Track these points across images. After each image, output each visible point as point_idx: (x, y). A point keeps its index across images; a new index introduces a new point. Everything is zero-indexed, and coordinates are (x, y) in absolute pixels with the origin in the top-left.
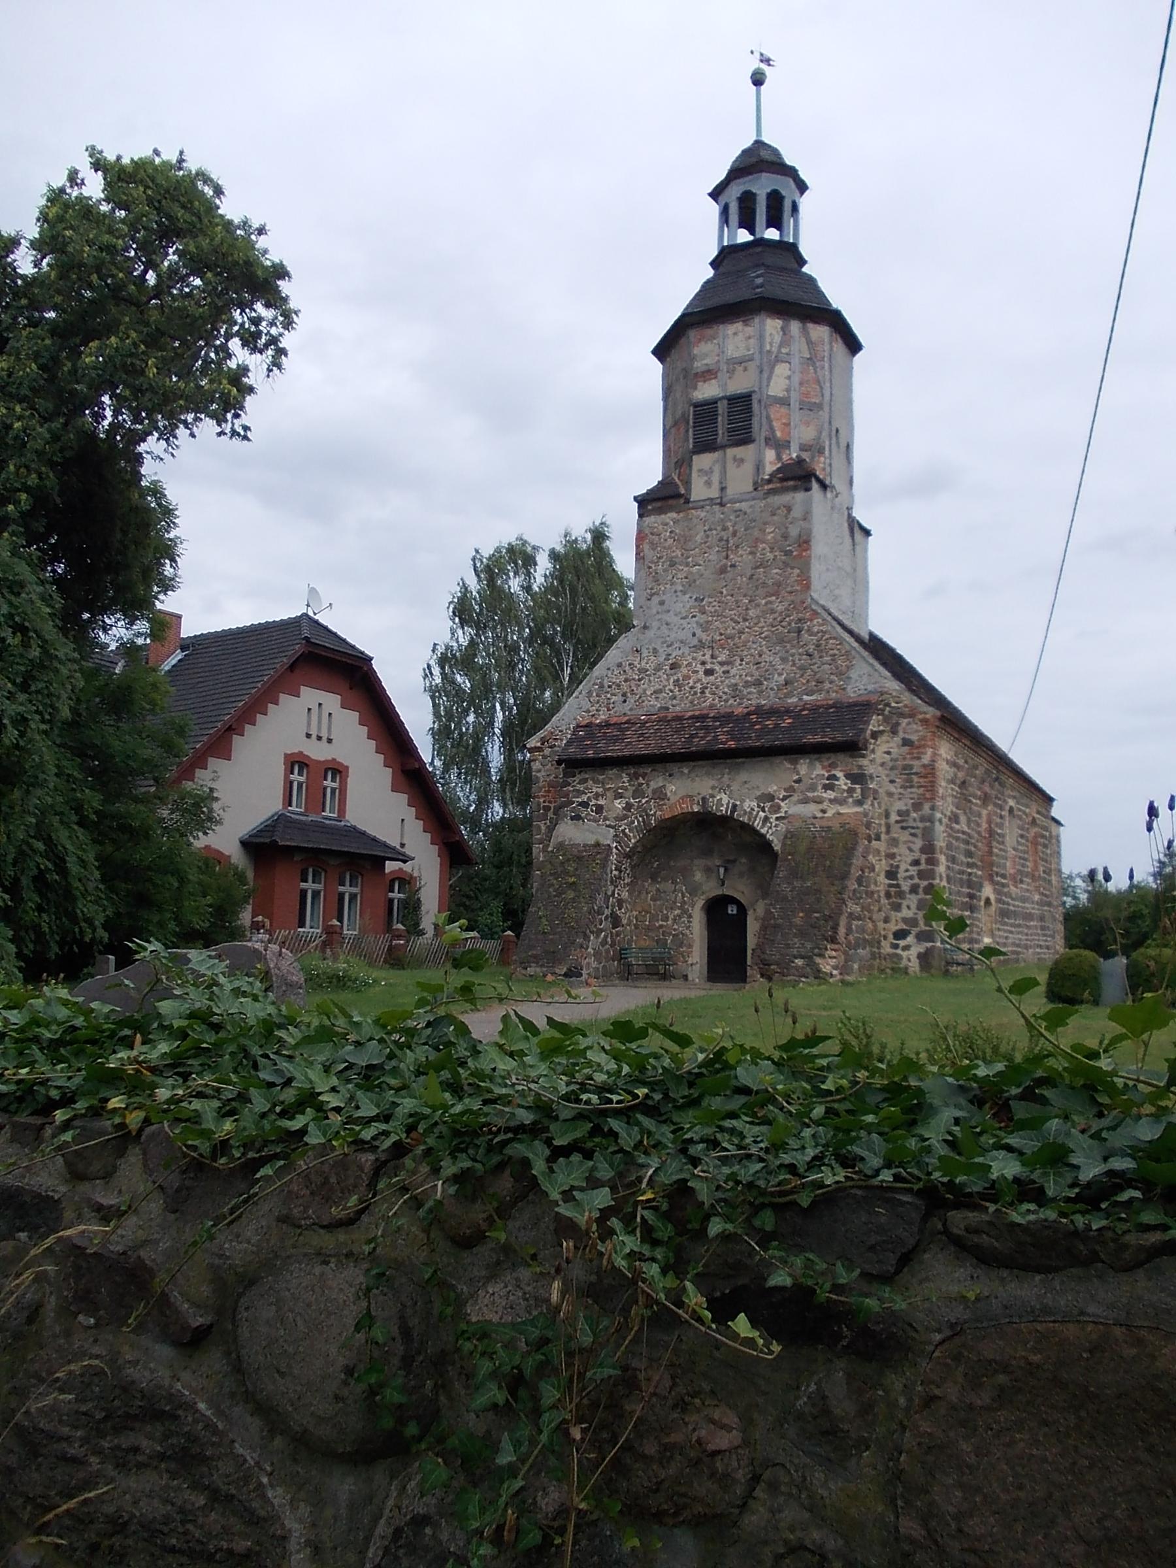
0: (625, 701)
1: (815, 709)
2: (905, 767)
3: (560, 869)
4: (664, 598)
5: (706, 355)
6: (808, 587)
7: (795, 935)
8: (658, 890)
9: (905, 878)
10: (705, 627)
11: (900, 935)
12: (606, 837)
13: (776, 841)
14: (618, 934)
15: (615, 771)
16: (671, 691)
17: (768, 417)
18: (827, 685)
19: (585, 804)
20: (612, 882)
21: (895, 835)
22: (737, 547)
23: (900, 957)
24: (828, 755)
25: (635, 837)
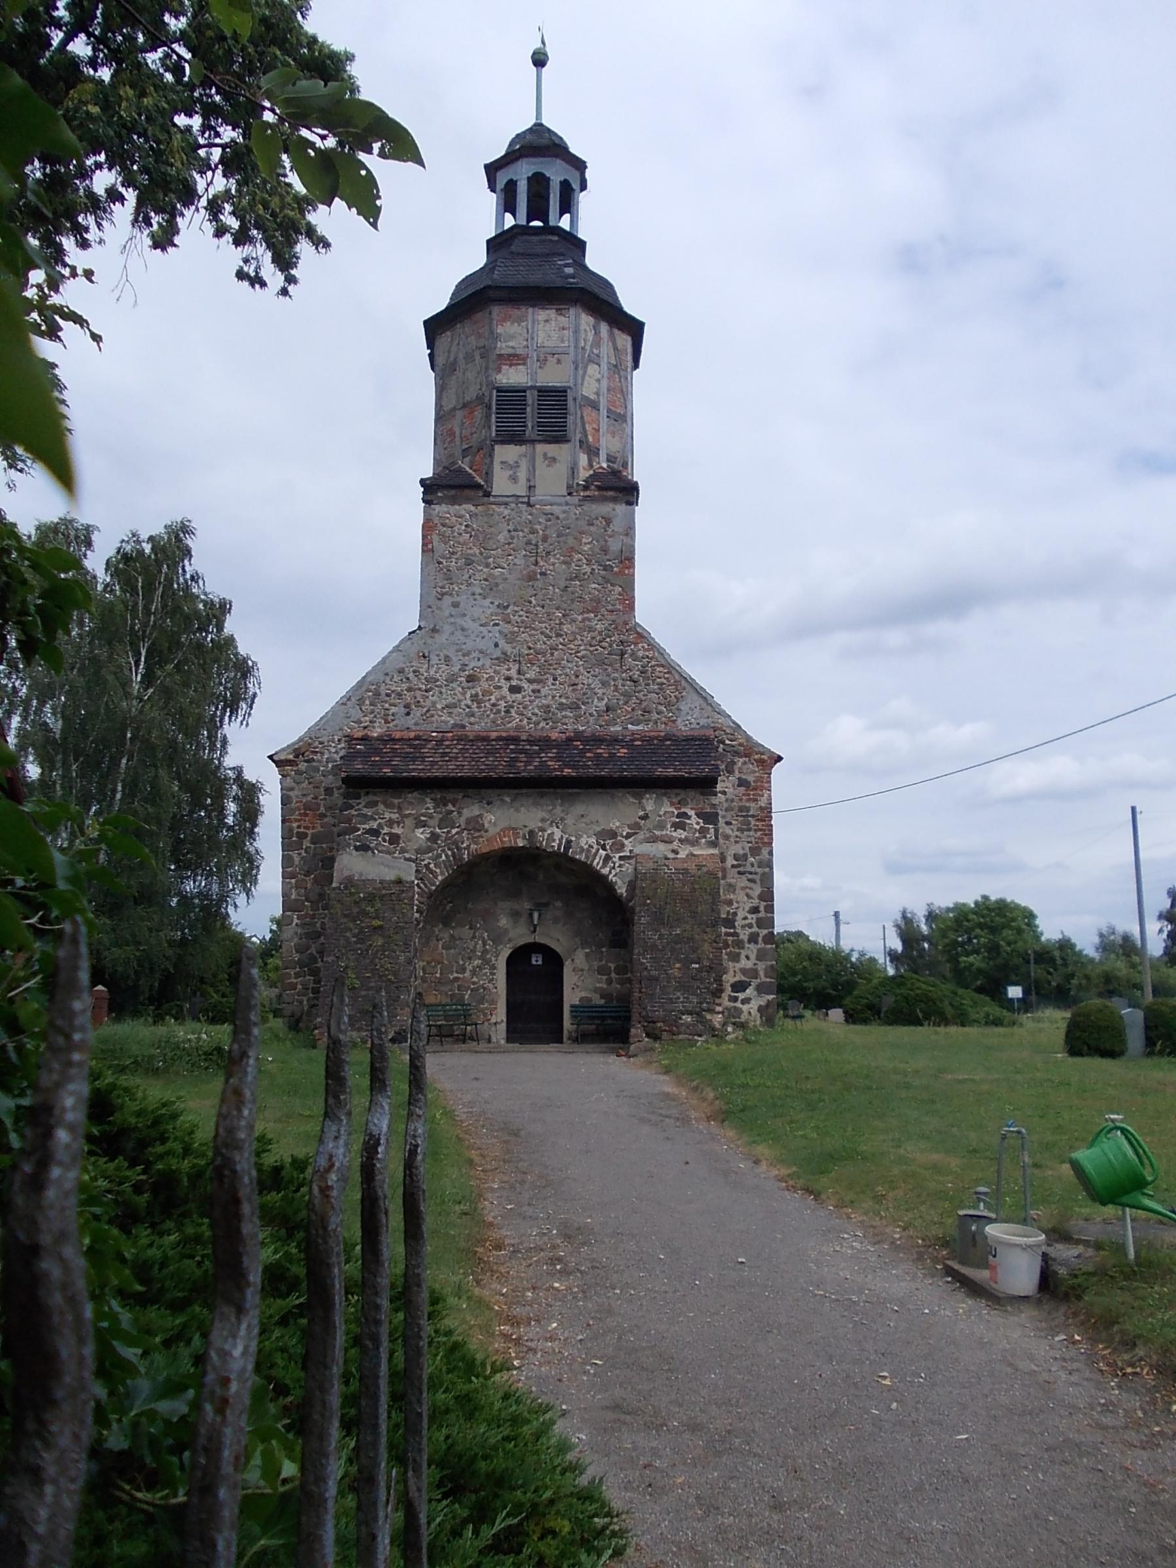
0: (408, 714)
1: (647, 740)
2: (741, 809)
3: (355, 910)
4: (458, 599)
5: (512, 337)
6: (631, 607)
7: (676, 989)
8: (452, 936)
9: (743, 927)
10: (511, 638)
11: (739, 987)
12: (410, 875)
13: (619, 882)
15: (415, 794)
16: (469, 707)
17: (582, 417)
18: (655, 716)
19: (375, 833)
21: (733, 881)
22: (548, 553)
23: (740, 1011)
24: (677, 791)
25: (442, 873)
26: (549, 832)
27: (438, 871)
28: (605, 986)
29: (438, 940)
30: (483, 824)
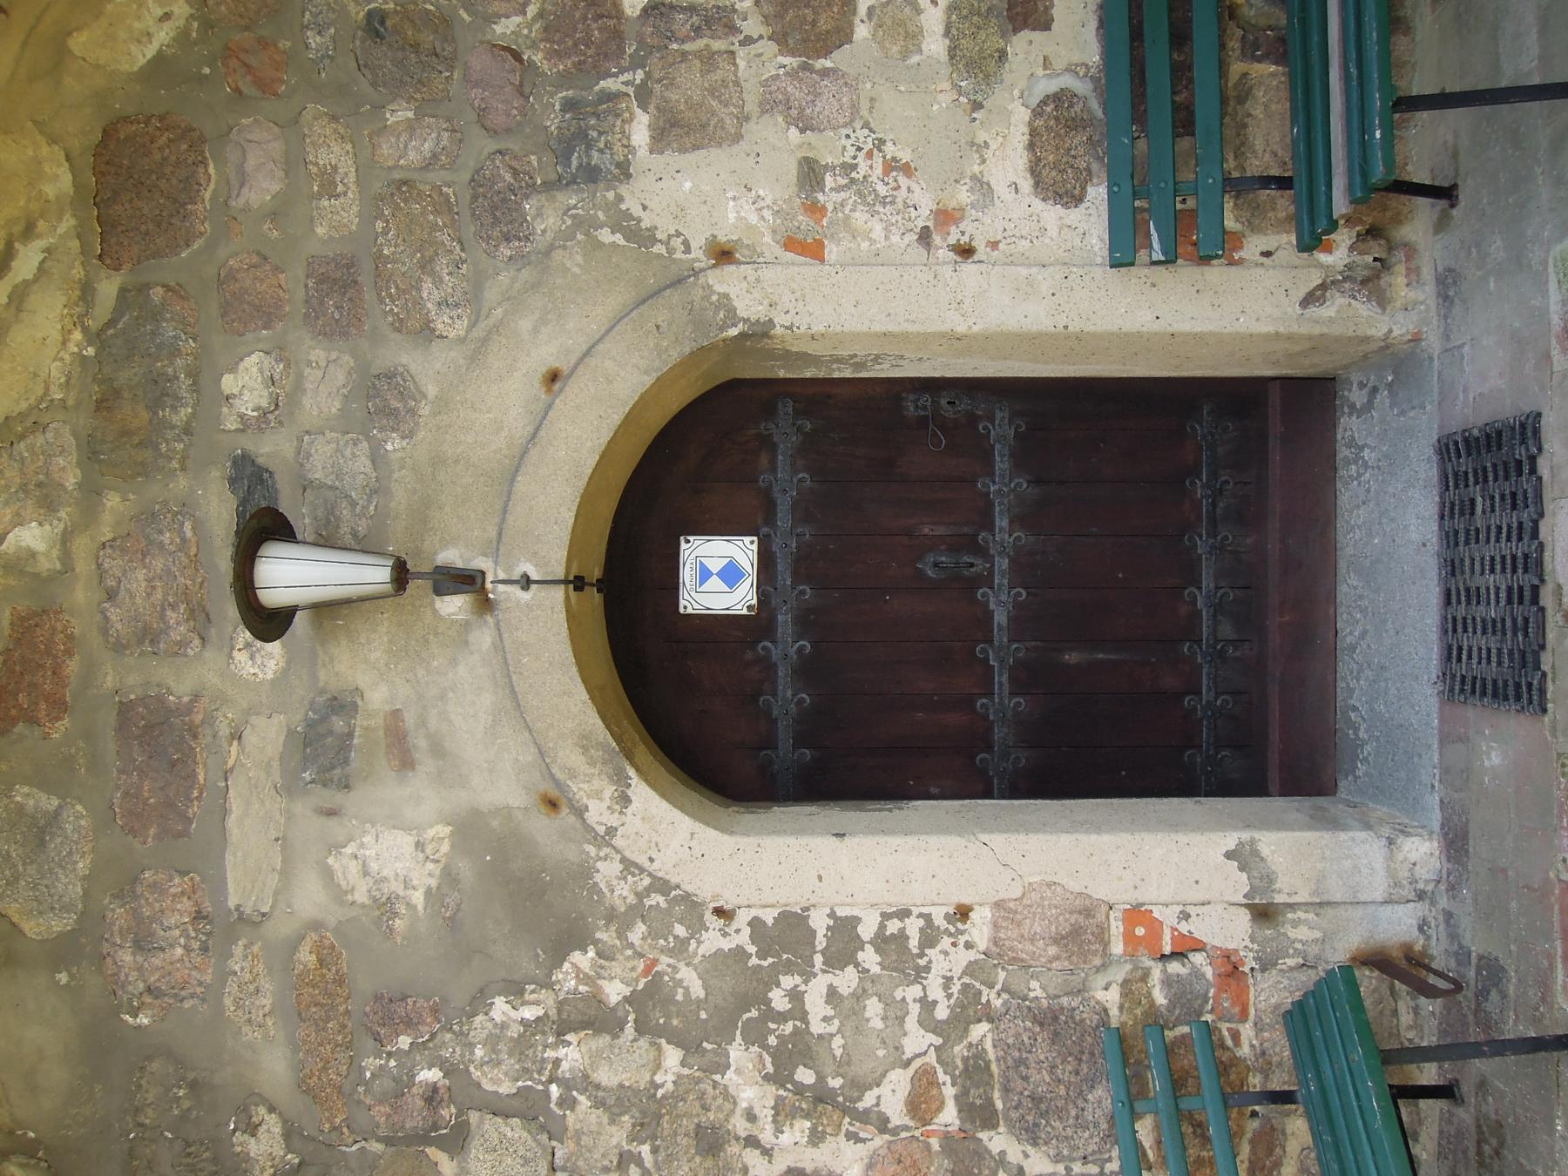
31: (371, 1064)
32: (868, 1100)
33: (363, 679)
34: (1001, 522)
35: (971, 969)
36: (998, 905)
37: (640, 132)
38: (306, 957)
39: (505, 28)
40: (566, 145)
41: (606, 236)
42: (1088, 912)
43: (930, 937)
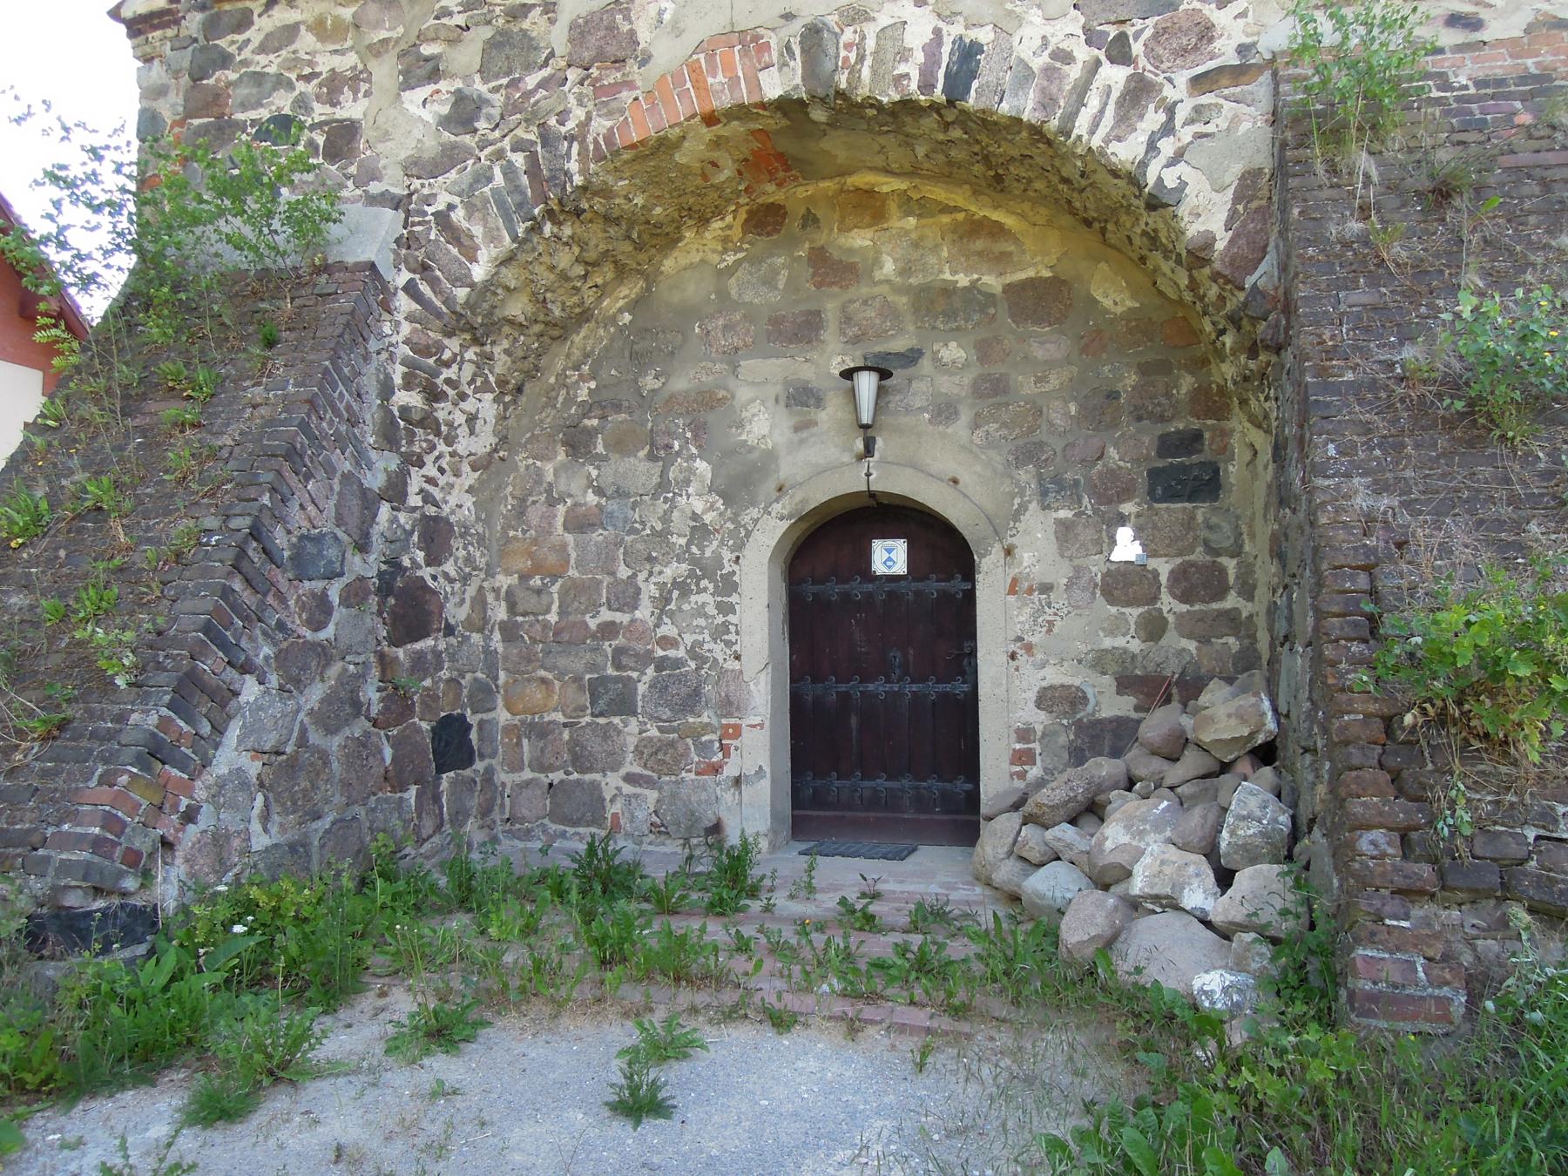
14: (420, 664)
20: (389, 436)
26: (884, 20)
27: (477, 231)
28: (1135, 646)
29: (552, 503)
30: (632, 36)
31: (681, 422)
32: (666, 620)
33: (830, 410)
34: (915, 688)
35: (715, 660)
36: (741, 672)
37: (1064, 514)
38: (721, 394)
39: (1112, 452)
40: (1058, 481)
41: (1017, 501)
42: (738, 708)
43: (729, 644)
